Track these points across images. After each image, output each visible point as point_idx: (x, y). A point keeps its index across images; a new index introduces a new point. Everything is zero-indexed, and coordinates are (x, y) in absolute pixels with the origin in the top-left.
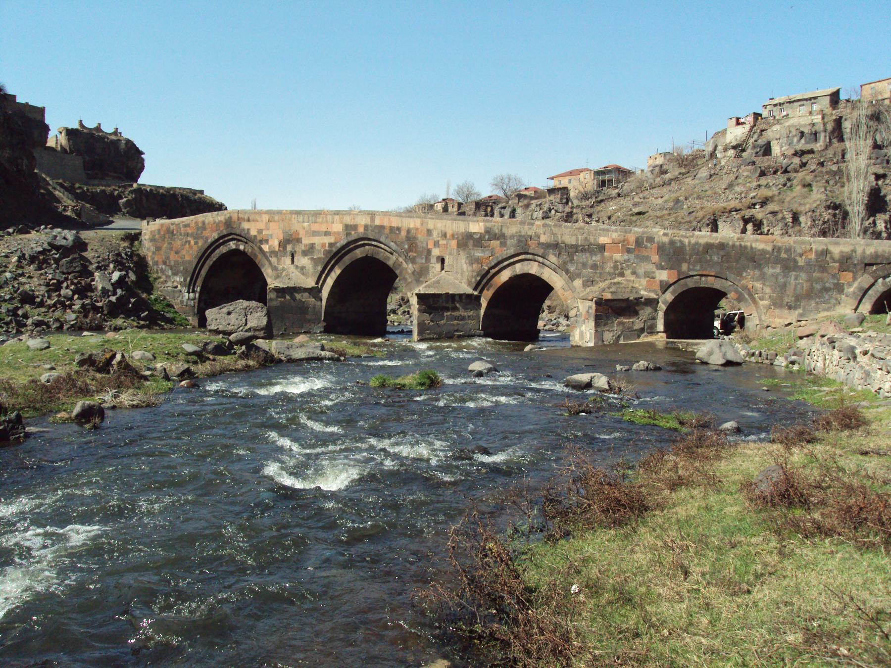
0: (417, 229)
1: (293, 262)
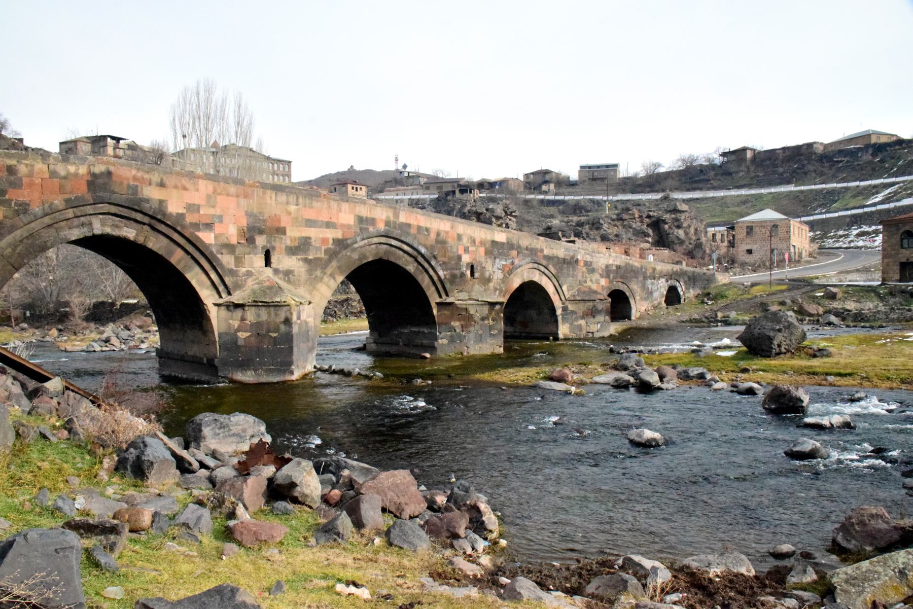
0: (447, 233)
1: (268, 263)
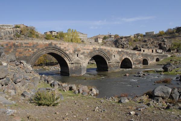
1: (78, 56)
